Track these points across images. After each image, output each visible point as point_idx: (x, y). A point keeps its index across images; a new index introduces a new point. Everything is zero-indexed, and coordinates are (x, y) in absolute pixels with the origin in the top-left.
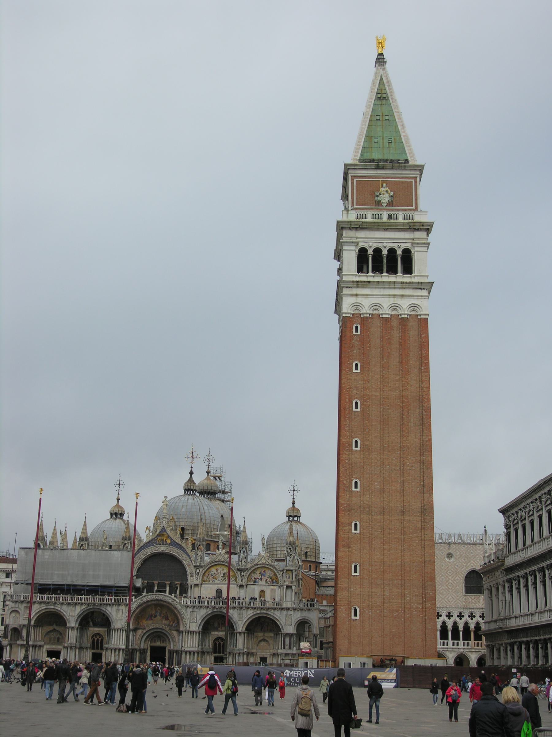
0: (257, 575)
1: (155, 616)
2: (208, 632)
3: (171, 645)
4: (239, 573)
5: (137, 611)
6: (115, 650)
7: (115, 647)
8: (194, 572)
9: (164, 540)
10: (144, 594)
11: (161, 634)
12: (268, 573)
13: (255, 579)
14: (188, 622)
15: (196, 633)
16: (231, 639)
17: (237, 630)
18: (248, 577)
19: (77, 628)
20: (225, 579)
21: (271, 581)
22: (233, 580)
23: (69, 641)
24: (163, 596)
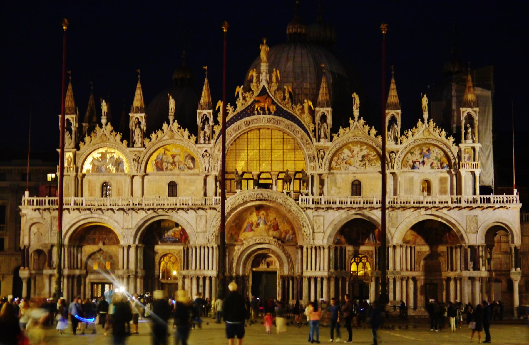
1: (258, 225)
3: (285, 269)
7: (198, 273)
8: (316, 155)
13: (414, 162)
15: (324, 248)
17: (389, 242)
18: (403, 161)
19: (137, 247)
20: (365, 164)
21: (439, 165)
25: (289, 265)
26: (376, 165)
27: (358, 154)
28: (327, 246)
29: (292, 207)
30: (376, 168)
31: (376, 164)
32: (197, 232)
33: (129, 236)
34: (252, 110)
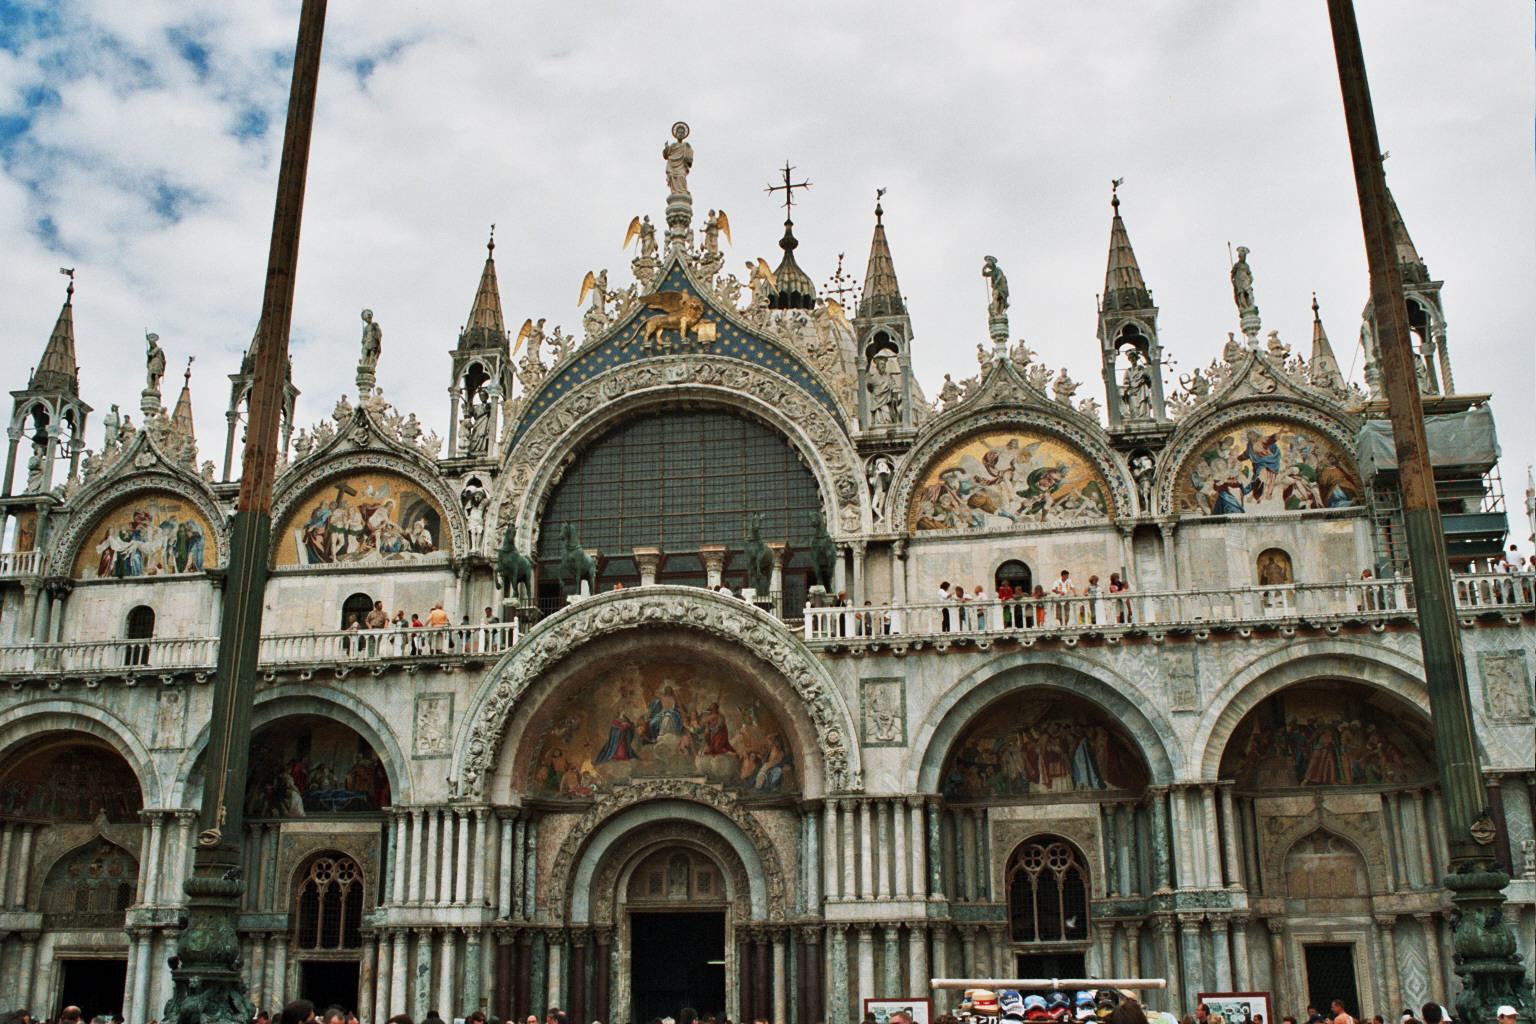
0: (1229, 467)
1: (652, 732)
2: (969, 812)
3: (754, 898)
4: (1121, 461)
5: (540, 699)
6: (412, 936)
7: (412, 917)
8: (860, 477)
9: (683, 325)
10: (574, 600)
11: (696, 840)
12: (1291, 450)
13: (1222, 489)
14: (850, 742)
15: (907, 809)
16: (1114, 842)
17: (1169, 771)
20: (1043, 503)
21: (1316, 491)
22: (1092, 504)
23: (148, 903)
24: (687, 601)
25: (767, 883)
26: (1083, 507)
27: (1013, 469)
28: (920, 801)
29: (778, 649)
30: (1081, 514)
31: (1080, 500)
32: (414, 758)
33: (172, 779)
34: (635, 342)
